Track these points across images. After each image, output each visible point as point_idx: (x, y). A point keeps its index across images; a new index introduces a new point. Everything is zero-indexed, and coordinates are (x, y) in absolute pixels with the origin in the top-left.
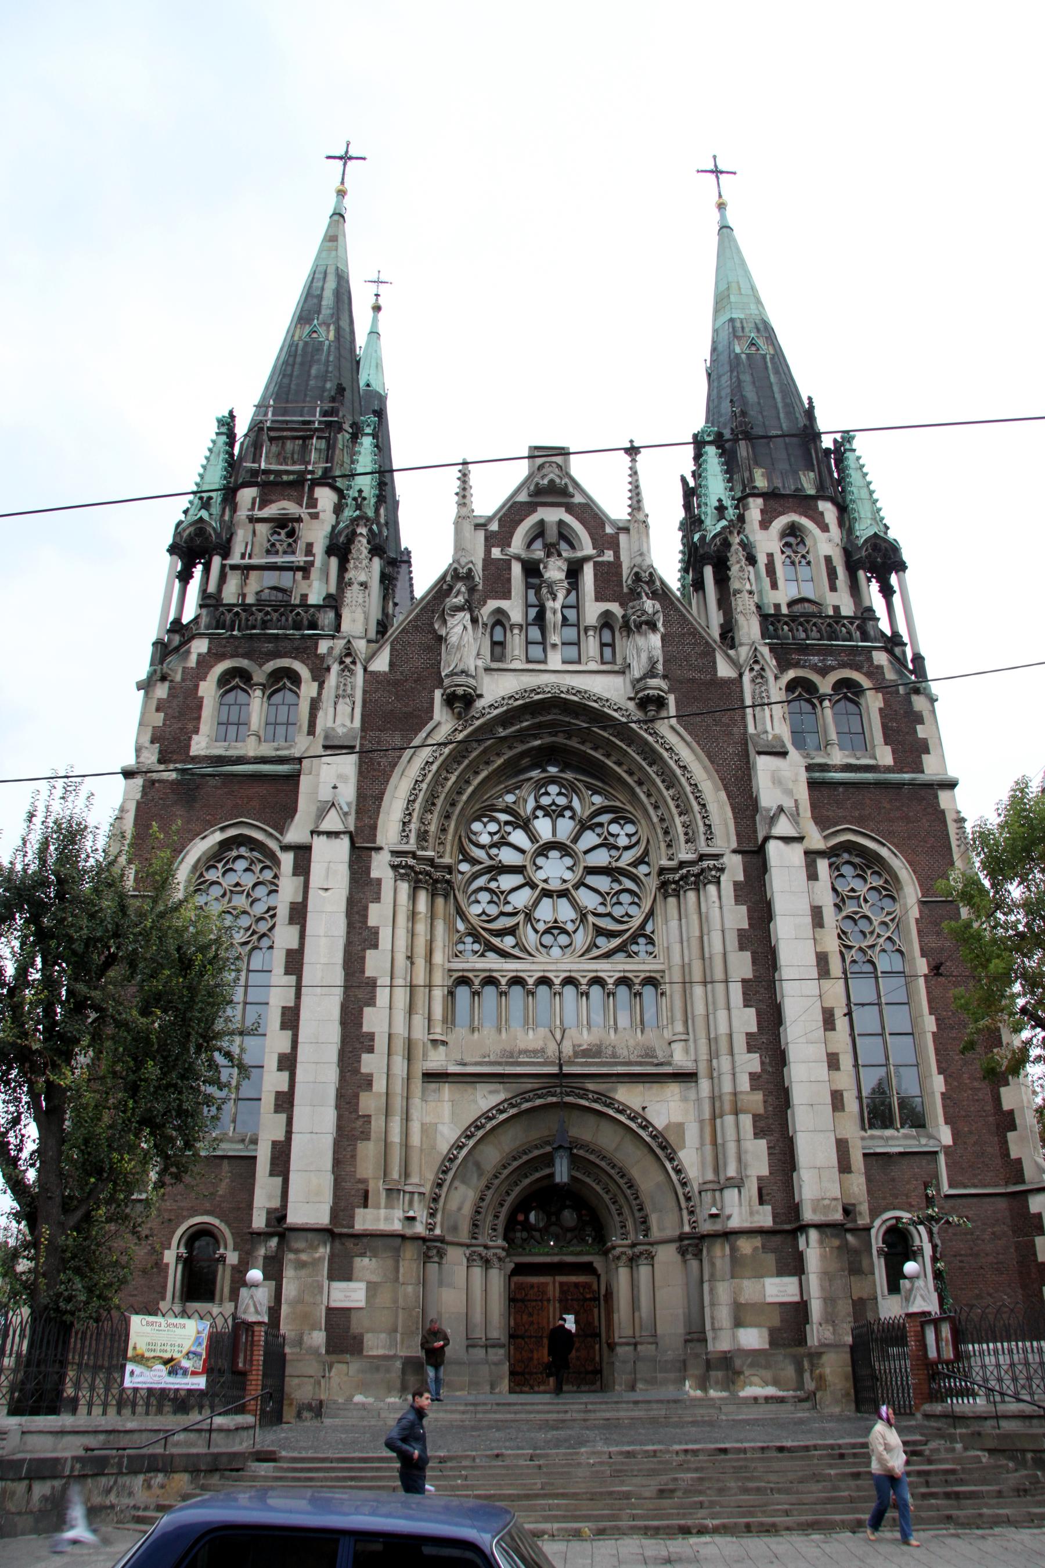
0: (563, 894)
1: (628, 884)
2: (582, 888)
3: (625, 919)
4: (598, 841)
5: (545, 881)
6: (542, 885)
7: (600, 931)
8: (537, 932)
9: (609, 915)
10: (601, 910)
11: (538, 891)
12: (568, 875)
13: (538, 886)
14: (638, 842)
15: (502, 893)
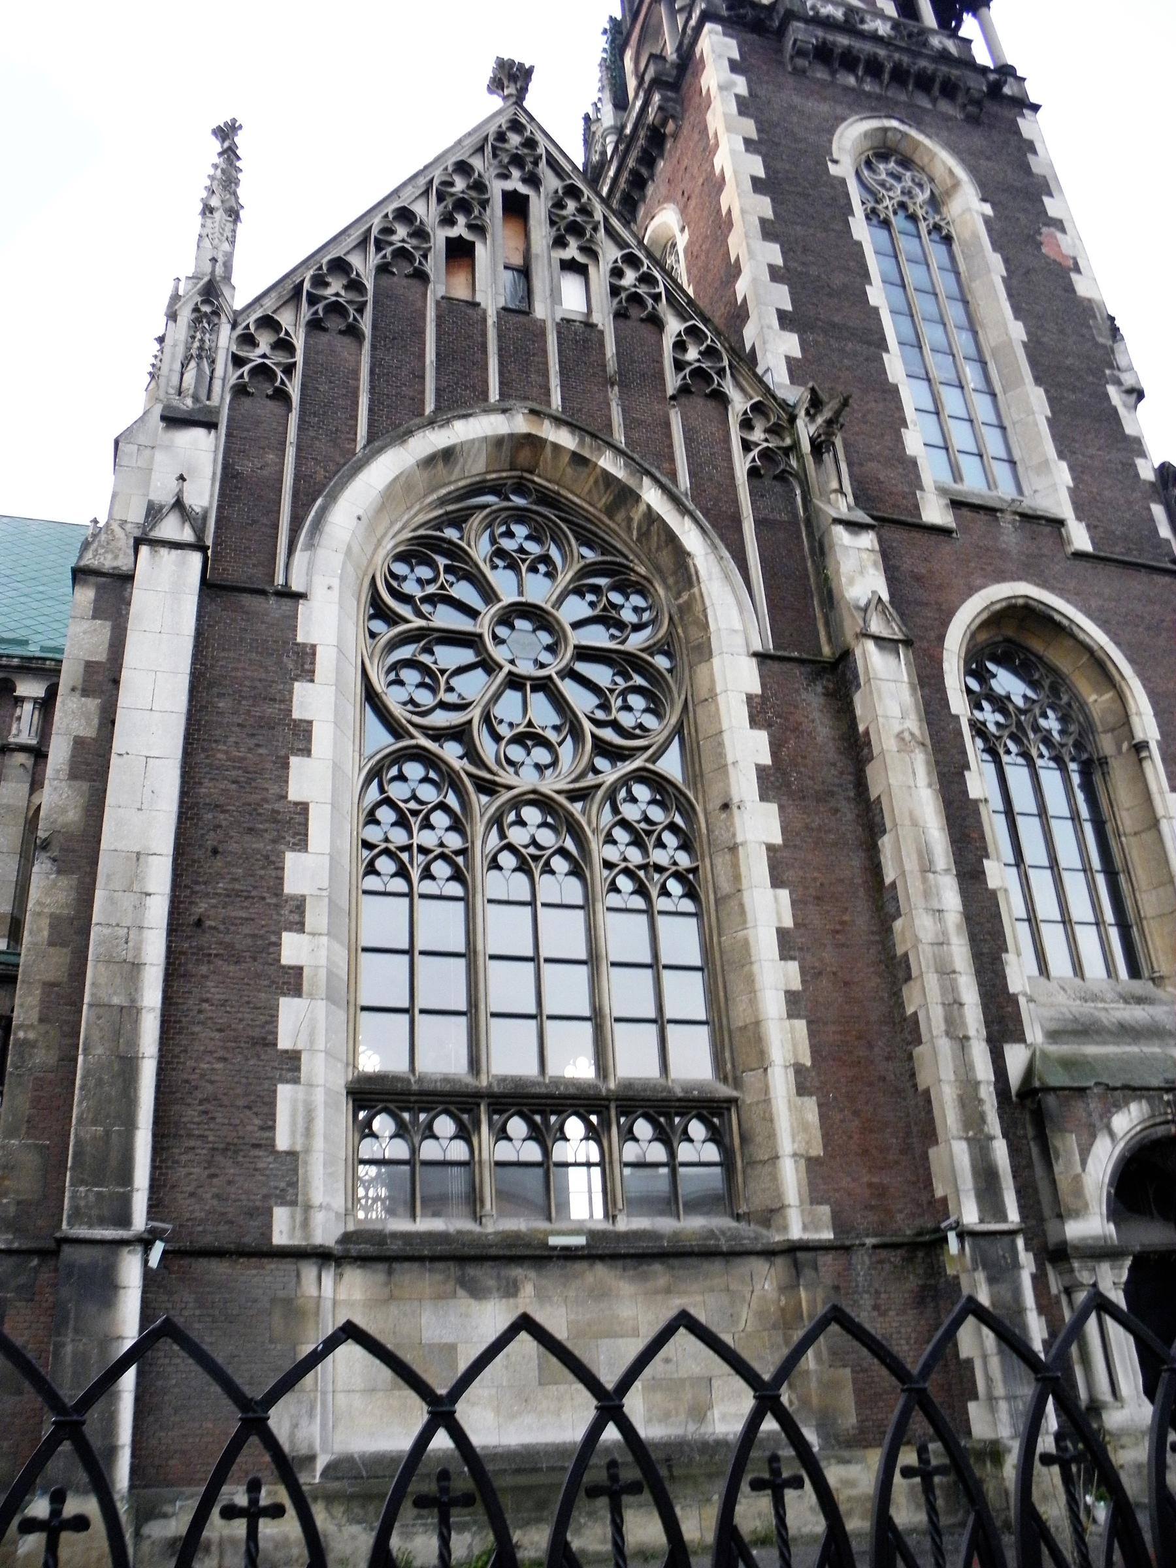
0: (544, 686)
1: (638, 680)
2: (568, 681)
3: (638, 731)
4: (597, 612)
5: (512, 662)
6: (508, 667)
7: (602, 748)
8: (497, 738)
9: (615, 725)
10: (600, 715)
11: (502, 675)
12: (545, 657)
13: (501, 668)
14: (653, 622)
15: (443, 672)
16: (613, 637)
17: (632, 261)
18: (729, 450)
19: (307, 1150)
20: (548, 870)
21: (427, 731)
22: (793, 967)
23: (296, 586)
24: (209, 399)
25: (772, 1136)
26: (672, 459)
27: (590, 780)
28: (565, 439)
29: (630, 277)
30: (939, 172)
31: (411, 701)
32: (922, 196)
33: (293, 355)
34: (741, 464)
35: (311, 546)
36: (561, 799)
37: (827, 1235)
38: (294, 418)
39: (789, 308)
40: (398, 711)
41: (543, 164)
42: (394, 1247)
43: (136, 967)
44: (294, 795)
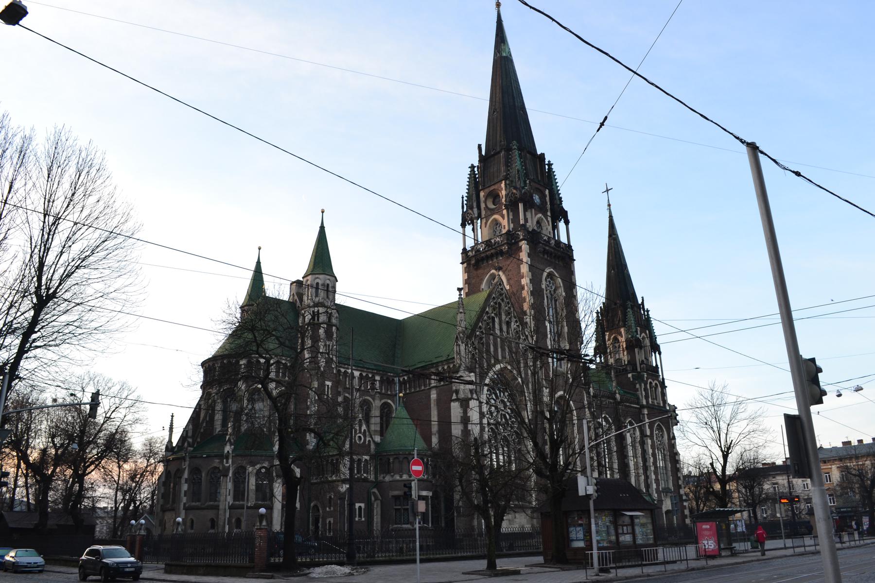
28: (509, 367)
30: (557, 282)
41: (504, 295)
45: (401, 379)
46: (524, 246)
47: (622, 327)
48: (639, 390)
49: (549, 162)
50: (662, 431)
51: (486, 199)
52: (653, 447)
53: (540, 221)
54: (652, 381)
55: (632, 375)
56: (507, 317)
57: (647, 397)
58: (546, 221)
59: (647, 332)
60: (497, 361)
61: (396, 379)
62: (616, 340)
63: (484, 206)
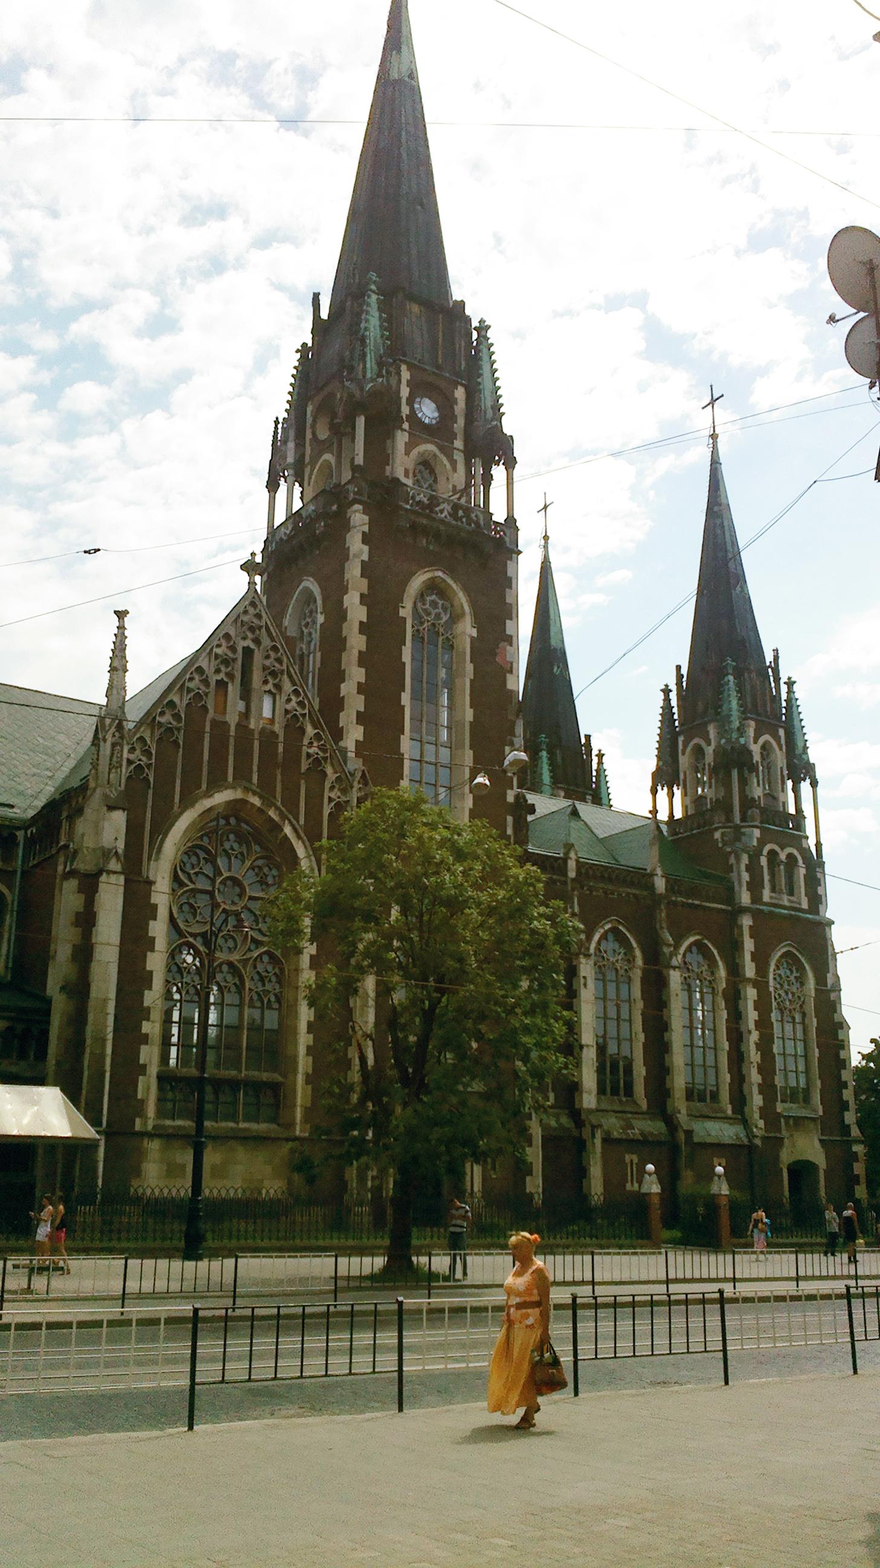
6: (223, 906)
7: (253, 940)
9: (260, 930)
12: (236, 899)
16: (263, 890)
17: (296, 692)
18: (322, 800)
19: (147, 1097)
20: (229, 991)
21: (191, 935)
22: (311, 1036)
23: (151, 878)
24: (120, 786)
25: (295, 1098)
26: (298, 806)
27: (248, 956)
28: (256, 801)
29: (293, 704)
30: (456, 603)
31: (187, 921)
32: (445, 618)
33: (151, 759)
34: (326, 811)
35: (157, 860)
36: (236, 963)
37: (307, 1135)
38: (151, 792)
39: (362, 710)
40: (182, 926)
42: (170, 1131)
43: (104, 1040)
44: (148, 968)
45: (29, 832)
46: (359, 519)
47: (710, 722)
48: (734, 868)
49: (481, 321)
50: (801, 968)
51: (314, 421)
52: (763, 1005)
53: (433, 464)
54: (777, 848)
55: (723, 834)
56: (266, 682)
57: (755, 886)
58: (446, 462)
59: (781, 732)
60: (217, 782)
61: (20, 834)
62: (699, 752)
63: (311, 437)
